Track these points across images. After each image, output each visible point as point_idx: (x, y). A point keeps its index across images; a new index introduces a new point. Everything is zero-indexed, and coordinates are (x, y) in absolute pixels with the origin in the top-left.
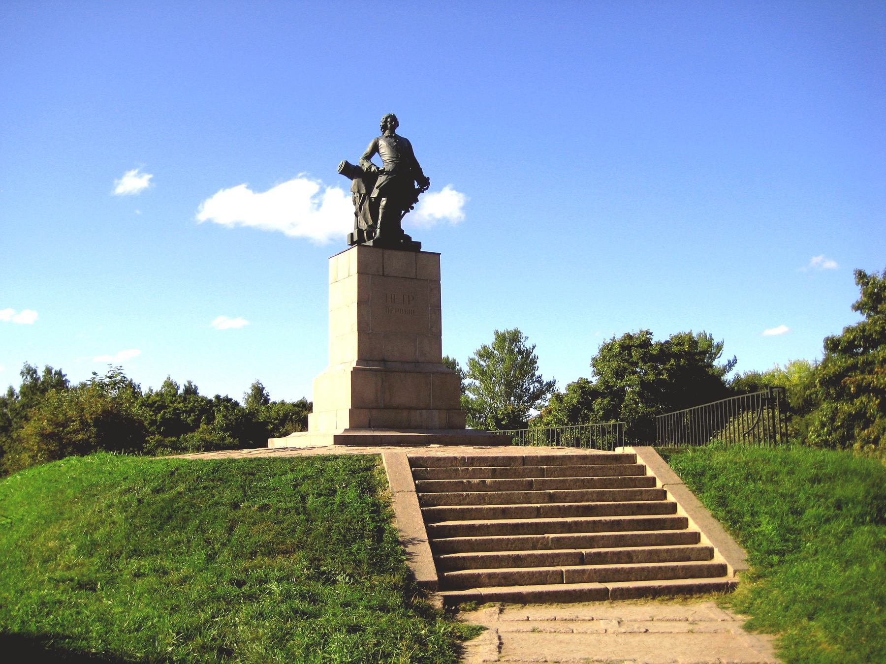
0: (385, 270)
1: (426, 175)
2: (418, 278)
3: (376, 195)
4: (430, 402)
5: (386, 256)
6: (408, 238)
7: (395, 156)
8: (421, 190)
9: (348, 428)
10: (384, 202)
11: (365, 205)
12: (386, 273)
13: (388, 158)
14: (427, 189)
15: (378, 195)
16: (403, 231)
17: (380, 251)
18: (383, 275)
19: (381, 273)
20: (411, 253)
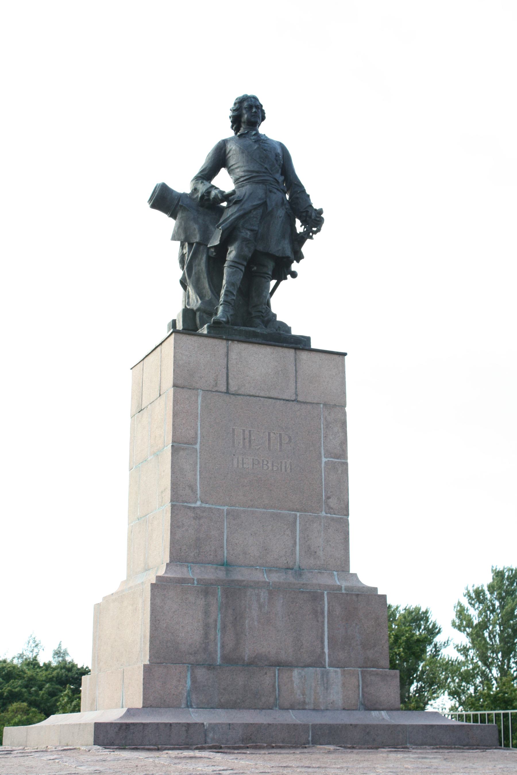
0: (230, 381)
1: (316, 206)
2: (300, 399)
3: (217, 242)
4: (323, 653)
5: (233, 355)
6: (284, 328)
7: (256, 168)
8: (306, 236)
9: (140, 705)
10: (232, 253)
11: (199, 265)
12: (232, 389)
13: (242, 174)
14: (319, 230)
15: (220, 241)
16: (275, 316)
17: (220, 345)
18: (227, 392)
19: (224, 389)
20: (286, 350)
